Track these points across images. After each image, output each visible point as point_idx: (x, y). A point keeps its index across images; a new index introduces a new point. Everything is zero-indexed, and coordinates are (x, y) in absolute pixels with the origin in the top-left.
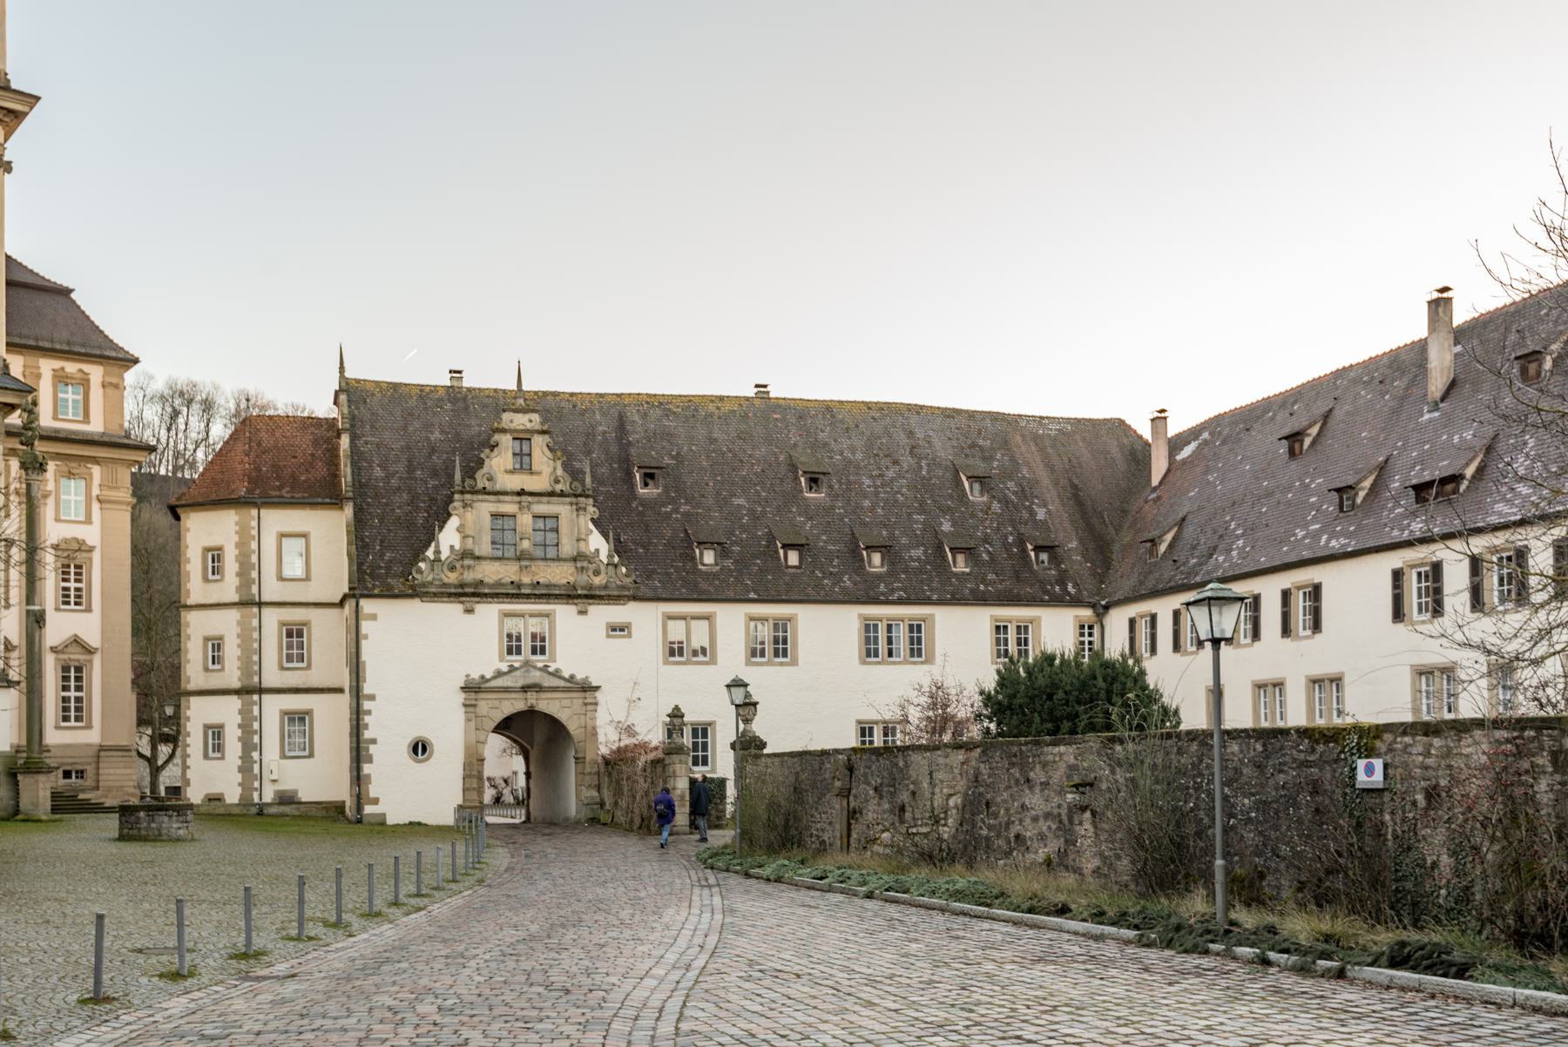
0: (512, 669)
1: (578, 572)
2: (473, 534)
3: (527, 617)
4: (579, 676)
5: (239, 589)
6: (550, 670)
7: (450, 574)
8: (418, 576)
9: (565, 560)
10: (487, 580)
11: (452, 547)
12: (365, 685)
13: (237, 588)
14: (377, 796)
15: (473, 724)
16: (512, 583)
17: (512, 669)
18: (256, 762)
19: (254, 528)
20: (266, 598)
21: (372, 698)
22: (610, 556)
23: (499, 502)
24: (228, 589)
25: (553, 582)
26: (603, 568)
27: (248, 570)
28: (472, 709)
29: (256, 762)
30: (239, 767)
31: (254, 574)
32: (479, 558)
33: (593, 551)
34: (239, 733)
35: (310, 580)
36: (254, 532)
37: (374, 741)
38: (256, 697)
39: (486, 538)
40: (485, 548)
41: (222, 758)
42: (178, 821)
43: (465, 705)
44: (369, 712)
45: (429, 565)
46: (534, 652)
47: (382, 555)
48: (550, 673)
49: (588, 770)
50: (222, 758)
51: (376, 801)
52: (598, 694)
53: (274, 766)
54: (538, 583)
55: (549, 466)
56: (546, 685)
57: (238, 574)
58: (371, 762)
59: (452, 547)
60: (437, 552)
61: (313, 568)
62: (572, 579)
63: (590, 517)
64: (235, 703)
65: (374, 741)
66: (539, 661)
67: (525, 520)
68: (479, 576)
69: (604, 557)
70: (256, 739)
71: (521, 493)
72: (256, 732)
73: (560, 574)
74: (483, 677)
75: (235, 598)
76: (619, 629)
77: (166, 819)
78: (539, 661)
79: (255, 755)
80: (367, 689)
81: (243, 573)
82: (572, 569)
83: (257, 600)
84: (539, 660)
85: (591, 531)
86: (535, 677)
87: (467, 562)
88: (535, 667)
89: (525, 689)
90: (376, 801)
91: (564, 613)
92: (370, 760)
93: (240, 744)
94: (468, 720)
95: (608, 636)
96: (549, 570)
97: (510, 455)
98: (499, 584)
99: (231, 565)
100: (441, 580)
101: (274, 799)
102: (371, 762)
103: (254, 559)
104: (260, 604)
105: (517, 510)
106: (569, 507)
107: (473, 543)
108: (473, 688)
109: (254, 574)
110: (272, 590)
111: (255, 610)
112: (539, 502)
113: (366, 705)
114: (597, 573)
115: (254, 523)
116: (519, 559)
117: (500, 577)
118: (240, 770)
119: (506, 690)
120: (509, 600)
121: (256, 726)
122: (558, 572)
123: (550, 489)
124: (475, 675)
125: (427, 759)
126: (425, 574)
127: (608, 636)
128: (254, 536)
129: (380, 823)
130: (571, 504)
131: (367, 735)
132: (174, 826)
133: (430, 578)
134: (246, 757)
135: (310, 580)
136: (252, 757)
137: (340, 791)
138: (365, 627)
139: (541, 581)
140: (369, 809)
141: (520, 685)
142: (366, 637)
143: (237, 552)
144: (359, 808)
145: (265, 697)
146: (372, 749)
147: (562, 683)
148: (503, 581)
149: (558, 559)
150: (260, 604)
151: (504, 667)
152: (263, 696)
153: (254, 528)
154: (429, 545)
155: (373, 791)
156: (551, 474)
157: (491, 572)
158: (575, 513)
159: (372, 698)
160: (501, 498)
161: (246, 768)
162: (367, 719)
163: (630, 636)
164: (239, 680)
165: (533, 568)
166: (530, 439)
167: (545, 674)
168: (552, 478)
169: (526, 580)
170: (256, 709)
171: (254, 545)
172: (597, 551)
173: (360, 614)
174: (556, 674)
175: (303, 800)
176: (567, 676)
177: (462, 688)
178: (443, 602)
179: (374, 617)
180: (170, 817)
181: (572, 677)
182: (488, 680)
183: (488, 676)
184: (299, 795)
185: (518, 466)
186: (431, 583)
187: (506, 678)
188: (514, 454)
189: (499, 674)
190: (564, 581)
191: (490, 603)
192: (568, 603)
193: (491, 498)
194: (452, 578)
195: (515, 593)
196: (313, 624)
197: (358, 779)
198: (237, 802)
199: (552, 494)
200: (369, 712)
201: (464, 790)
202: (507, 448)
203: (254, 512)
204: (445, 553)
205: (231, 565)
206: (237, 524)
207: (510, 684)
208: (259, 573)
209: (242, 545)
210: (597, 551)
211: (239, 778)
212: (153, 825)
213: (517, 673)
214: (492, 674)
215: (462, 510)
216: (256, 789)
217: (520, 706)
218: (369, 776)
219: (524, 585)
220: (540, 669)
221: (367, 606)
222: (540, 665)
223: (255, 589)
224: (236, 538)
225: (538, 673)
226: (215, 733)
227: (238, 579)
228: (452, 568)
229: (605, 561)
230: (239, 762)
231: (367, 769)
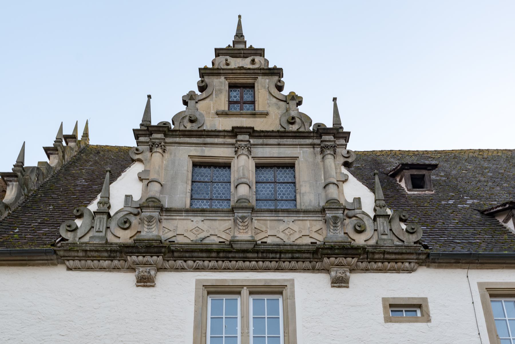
1: (328, 227)
2: (162, 183)
3: (245, 292)
8: (69, 236)
9: (306, 212)
11: (128, 197)
26: (369, 224)
32: (169, 210)
33: (350, 200)
55: (279, 108)
59: (128, 197)
60: (106, 203)
63: (343, 160)
82: (319, 225)
95: (388, 320)
96: (282, 227)
105: (233, 155)
106: (309, 150)
107: (161, 192)
116: (232, 211)
117: (202, 235)
120: (213, 263)
127: (388, 320)
130: (313, 145)
154: (95, 198)
156: (283, 115)
158: (319, 157)
163: (427, 318)
165: (256, 223)
166: (252, 87)
168: (284, 120)
172: (358, 200)
178: (102, 269)
191: (183, 269)
192: (313, 270)
210: (358, 200)
215: (148, 154)
228: (125, 224)
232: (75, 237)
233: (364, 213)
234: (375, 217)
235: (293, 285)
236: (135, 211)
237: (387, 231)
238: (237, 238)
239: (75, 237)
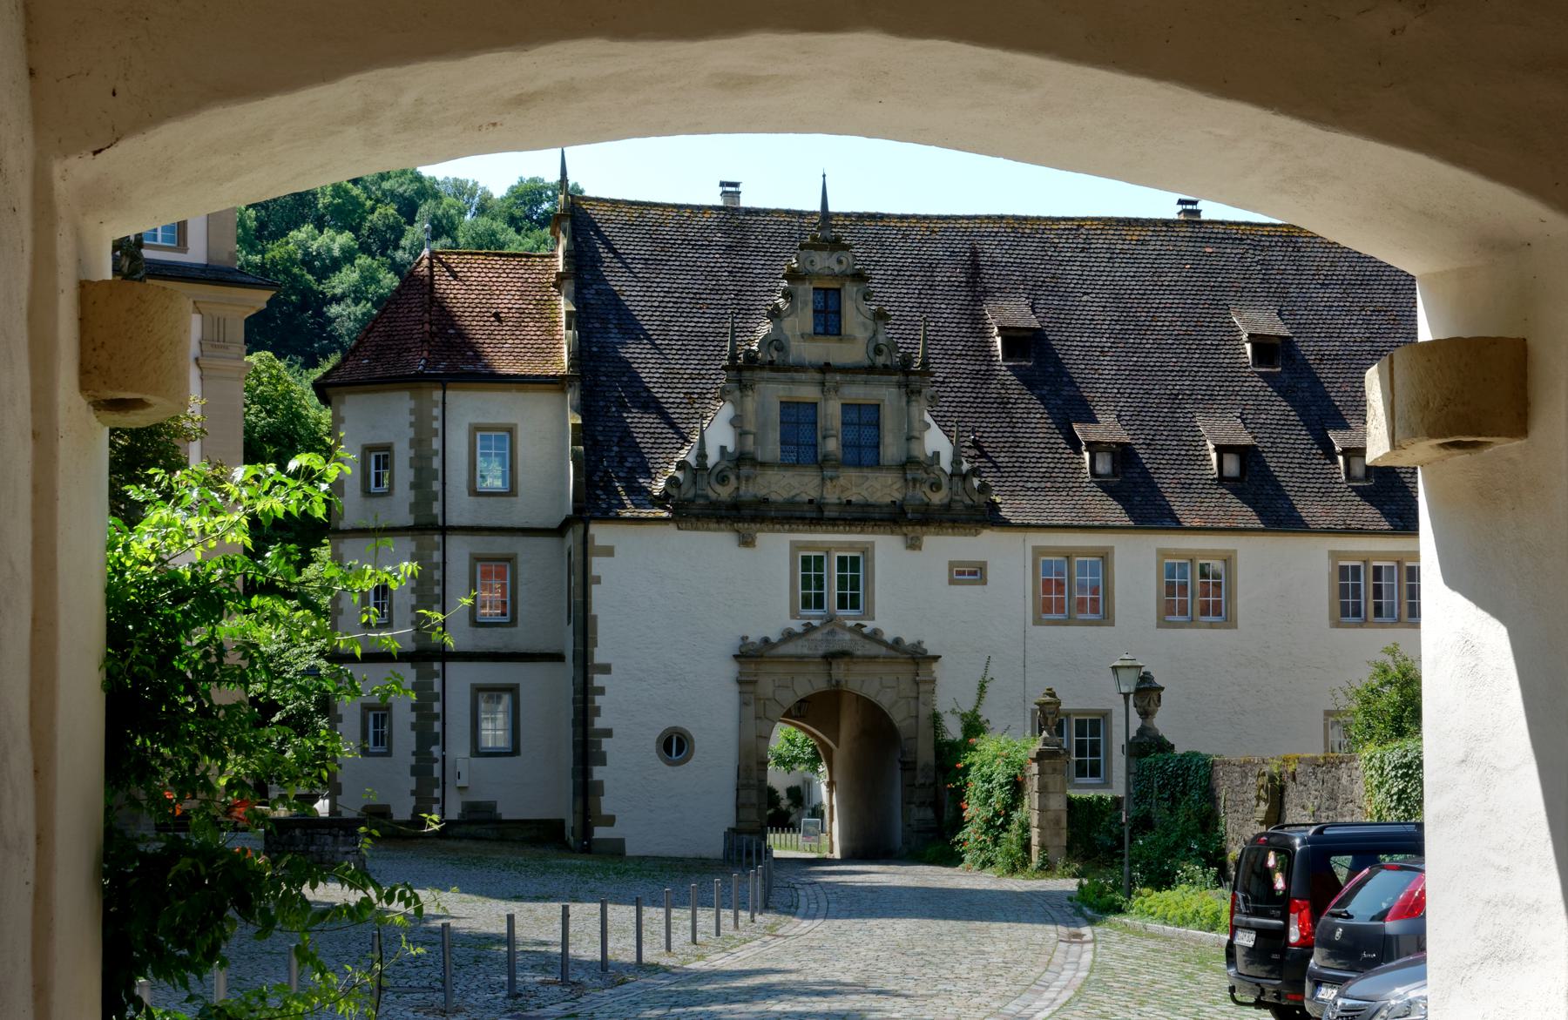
0: (809, 628)
4: (908, 639)
5: (415, 507)
6: (865, 630)
7: (719, 489)
9: (889, 468)
10: (773, 497)
11: (723, 449)
12: (596, 651)
13: (411, 505)
14: (612, 813)
15: (751, 710)
16: (811, 501)
17: (809, 628)
18: (436, 761)
19: (436, 418)
20: (453, 519)
21: (606, 669)
22: (956, 462)
23: (793, 381)
24: (400, 509)
25: (871, 500)
26: (944, 480)
27: (427, 478)
28: (750, 688)
29: (436, 761)
30: (413, 767)
31: (437, 486)
32: (763, 464)
33: (929, 453)
34: (413, 717)
35: (516, 495)
36: (437, 425)
37: (608, 733)
38: (437, 666)
39: (774, 436)
40: (771, 448)
41: (388, 754)
42: (345, 844)
43: (740, 682)
44: (601, 691)
45: (690, 475)
46: (842, 605)
47: (622, 460)
48: (866, 636)
49: (920, 780)
50: (388, 754)
51: (610, 821)
52: (935, 666)
53: (462, 767)
54: (849, 502)
55: (866, 329)
56: (859, 653)
57: (414, 486)
58: (604, 763)
59: (723, 449)
61: (521, 477)
62: (897, 496)
64: (408, 672)
65: (608, 733)
66: (848, 618)
67: (832, 411)
68: (762, 492)
69: (945, 463)
70: (437, 726)
71: (826, 368)
72: (436, 717)
73: (881, 488)
74: (766, 641)
75: (408, 519)
76: (974, 573)
77: (330, 839)
78: (848, 618)
79: (436, 750)
80: (599, 656)
81: (420, 484)
83: (440, 522)
84: (849, 617)
85: (928, 426)
86: (844, 640)
87: (745, 470)
88: (844, 627)
89: (830, 658)
90: (610, 821)
91: (886, 548)
92: (602, 760)
93: (414, 733)
94: (744, 704)
97: (809, 312)
98: (791, 503)
99: (403, 473)
100: (706, 497)
101: (462, 815)
102: (604, 763)
103: (436, 463)
104: (445, 530)
106: (894, 390)
108: (751, 656)
109: (437, 486)
110: (461, 509)
111: (437, 538)
112: (853, 382)
113: (598, 680)
114: (936, 486)
115: (437, 412)
117: (793, 493)
118: (415, 771)
119: (800, 659)
121: (437, 707)
122: (878, 486)
123: (867, 362)
124: (755, 636)
125: (686, 760)
126: (684, 488)
128: (436, 430)
129: (616, 849)
131: (599, 723)
132: (340, 849)
133: (690, 494)
134: (422, 752)
135: (516, 495)
136: (431, 753)
137: (557, 805)
138: (598, 565)
139: (854, 499)
140: (600, 832)
141: (821, 651)
142: (598, 580)
143: (412, 453)
144: (586, 830)
145: (449, 665)
146: (606, 744)
147: (883, 651)
148: (798, 499)
149: (876, 464)
150: (445, 530)
151: (797, 626)
152: (447, 664)
153: (436, 418)
155: (607, 805)
156: (871, 339)
157: (782, 485)
158: (904, 399)
159: (606, 669)
160: (796, 376)
161: (421, 769)
162: (599, 700)
164: (413, 641)
165: (842, 481)
166: (838, 291)
167: (857, 638)
169: (832, 496)
170: (437, 683)
171: (436, 444)
172: (937, 454)
173: (589, 545)
174: (875, 637)
175: (505, 817)
176: (890, 641)
177: (734, 656)
179: (609, 552)
180: (336, 837)
181: (898, 641)
182: (774, 646)
183: (774, 638)
184: (499, 810)
185: (820, 329)
186: (692, 501)
187: (800, 642)
188: (815, 311)
189: (789, 636)
190: (888, 500)
191: (779, 531)
192: (892, 533)
193: (780, 375)
194: (724, 493)
195: (814, 515)
196: (521, 559)
197: (586, 791)
198: (410, 818)
199: (871, 370)
200: (601, 691)
201: (739, 807)
202: (805, 303)
203: (437, 395)
204: (713, 457)
205: (403, 473)
206: (412, 412)
207: (806, 651)
208: (444, 484)
209: (418, 443)
210: (937, 454)
211: (412, 783)
212: (313, 848)
213: (817, 636)
214: (780, 637)
216: (436, 801)
217: (821, 685)
218: (600, 783)
219: (827, 504)
220: (851, 630)
221: (601, 534)
222: (850, 623)
223: (437, 508)
224: (411, 433)
225: (847, 636)
226: (378, 716)
227: (413, 492)
228: (723, 479)
229: (948, 469)
230: (413, 760)
231: (598, 773)
232: (679, 494)
233: (942, 470)
234: (952, 475)
235: (873, 547)
236: (731, 465)
237: (960, 491)
238: (826, 501)
239: (679, 494)
